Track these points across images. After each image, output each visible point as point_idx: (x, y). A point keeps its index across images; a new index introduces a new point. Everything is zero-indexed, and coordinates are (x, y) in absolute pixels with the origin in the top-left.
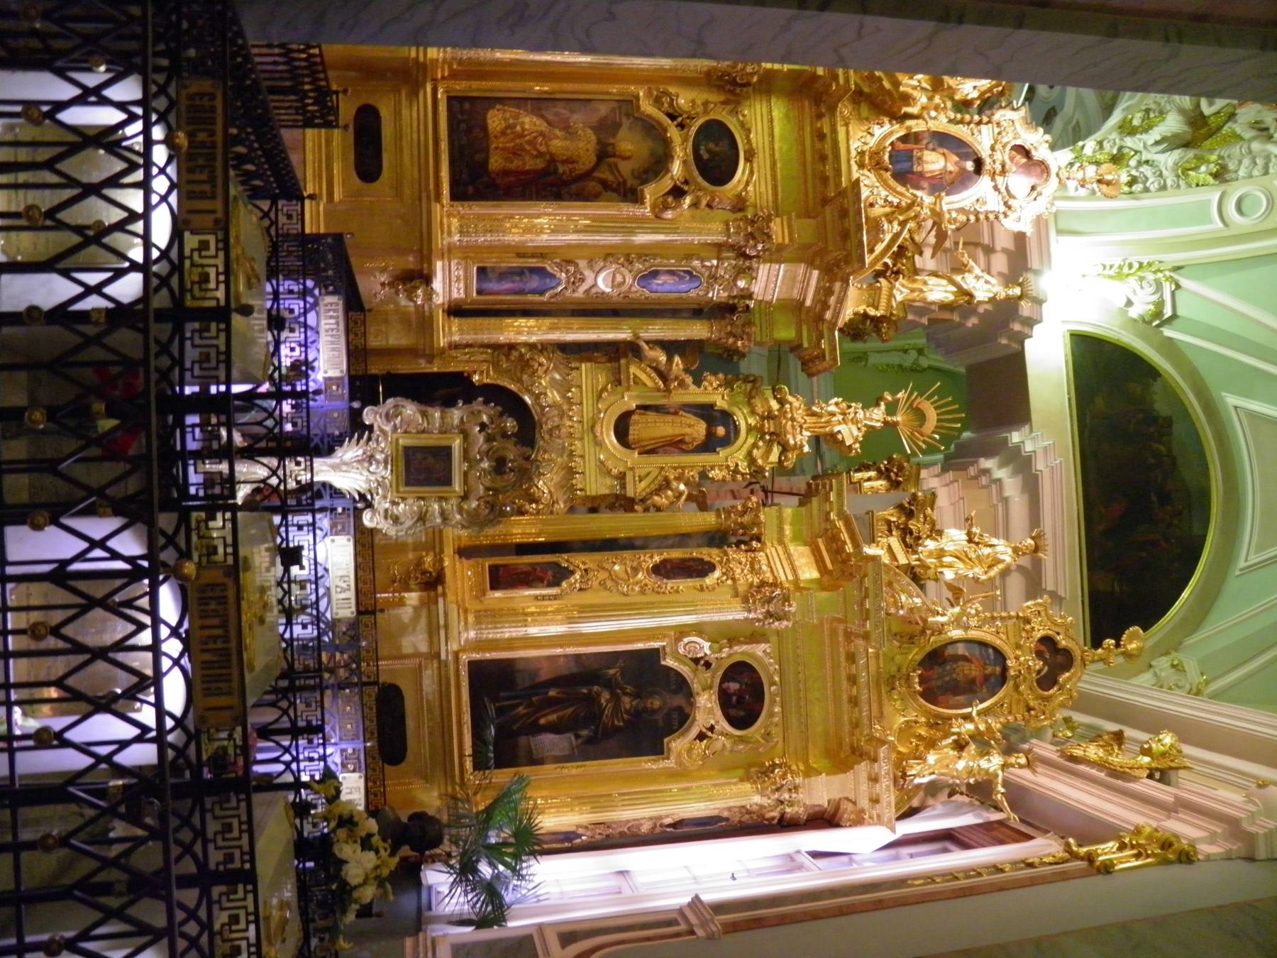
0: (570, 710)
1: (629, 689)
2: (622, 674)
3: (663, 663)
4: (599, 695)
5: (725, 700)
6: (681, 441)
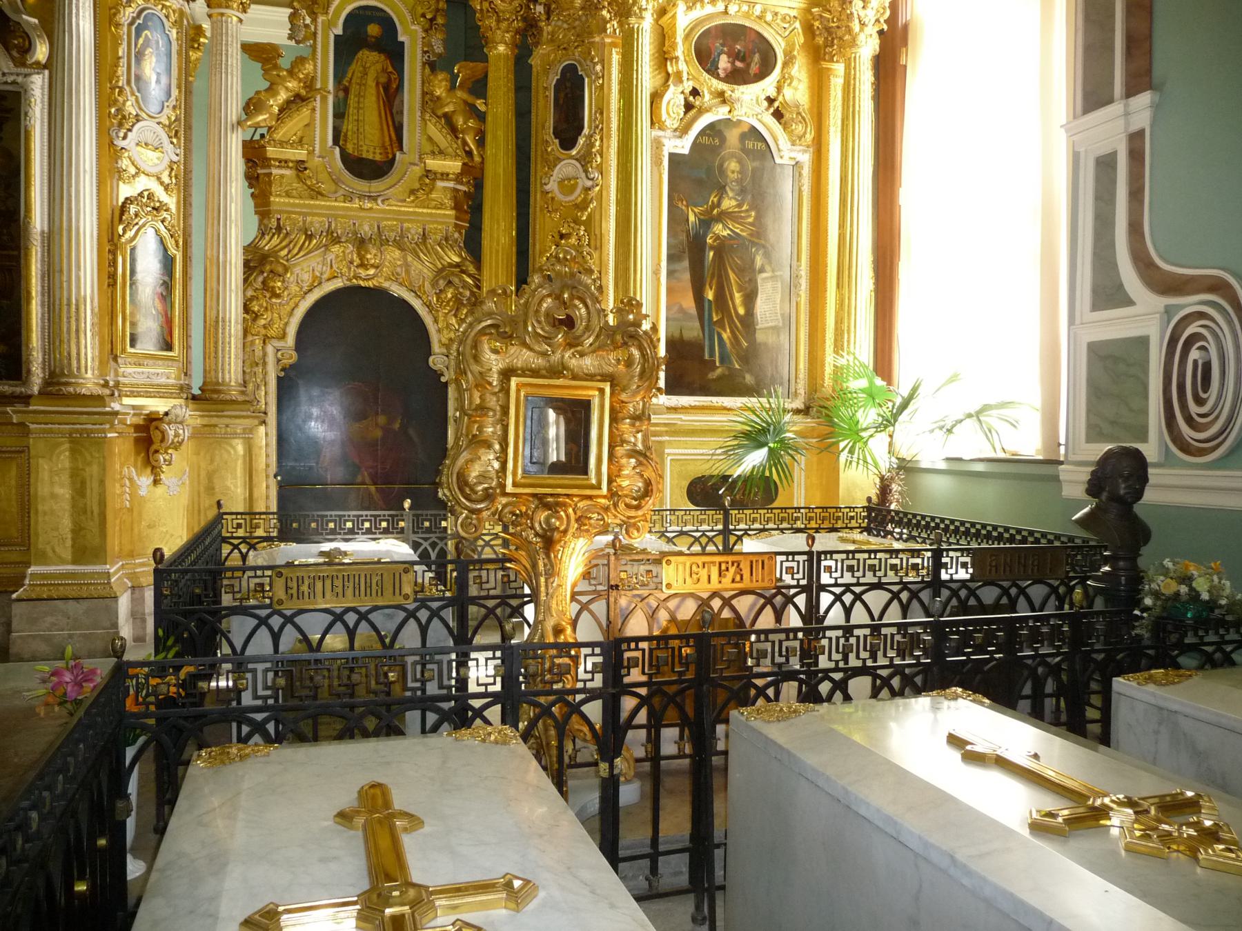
0: (732, 276)
1: (713, 199)
2: (695, 207)
3: (686, 151)
4: (718, 237)
5: (738, 77)
6: (386, 88)
